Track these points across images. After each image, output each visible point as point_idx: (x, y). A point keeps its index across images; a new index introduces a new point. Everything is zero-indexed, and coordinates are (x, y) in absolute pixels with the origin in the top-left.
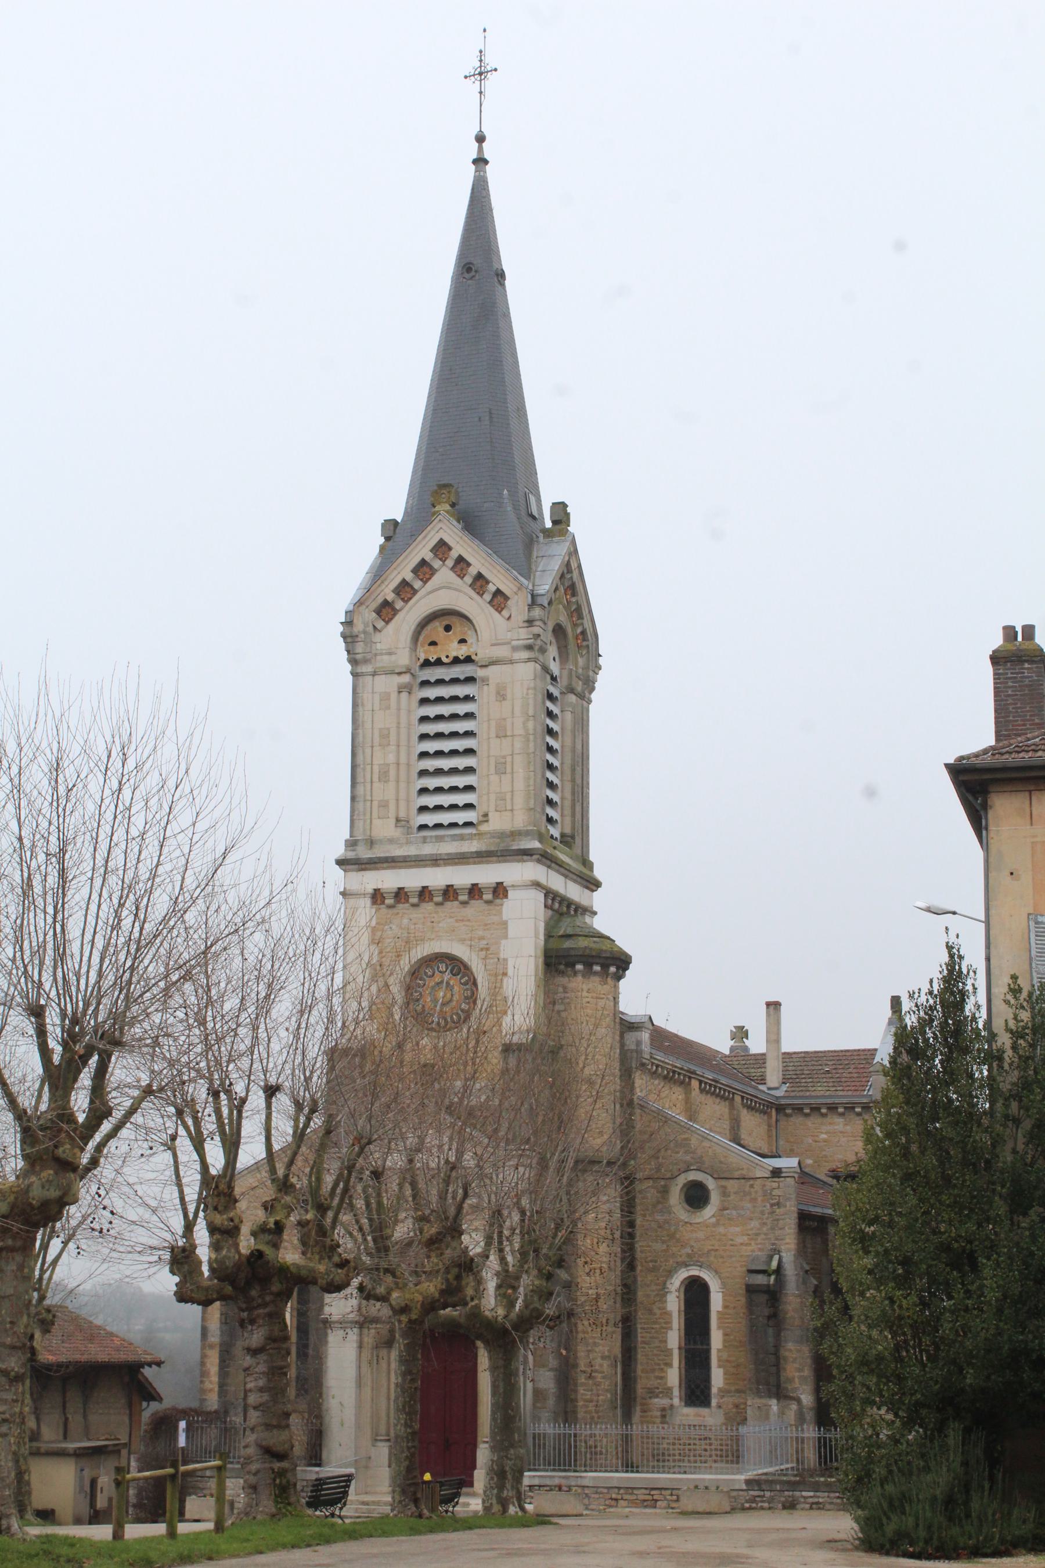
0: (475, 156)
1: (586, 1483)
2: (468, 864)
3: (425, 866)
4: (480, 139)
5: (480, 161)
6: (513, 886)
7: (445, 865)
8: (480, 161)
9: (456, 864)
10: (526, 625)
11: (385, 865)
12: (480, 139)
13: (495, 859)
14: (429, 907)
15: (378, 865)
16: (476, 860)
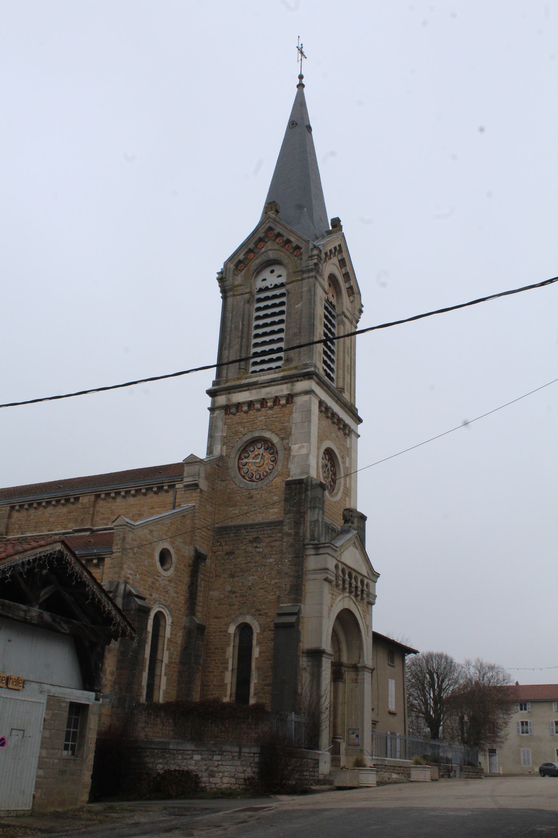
0: (298, 83)
1: (386, 763)
2: (344, 410)
3: (333, 399)
4: (301, 77)
5: (301, 86)
6: (355, 432)
7: (339, 405)
8: (301, 86)
9: (341, 407)
10: (359, 311)
11: (326, 388)
12: (301, 77)
13: (351, 414)
14: (330, 421)
15: (324, 386)
16: (348, 410)
